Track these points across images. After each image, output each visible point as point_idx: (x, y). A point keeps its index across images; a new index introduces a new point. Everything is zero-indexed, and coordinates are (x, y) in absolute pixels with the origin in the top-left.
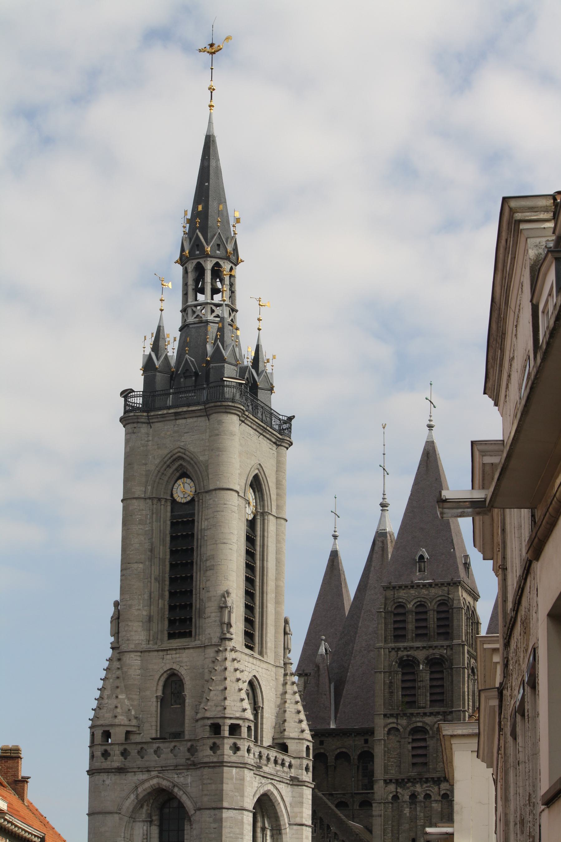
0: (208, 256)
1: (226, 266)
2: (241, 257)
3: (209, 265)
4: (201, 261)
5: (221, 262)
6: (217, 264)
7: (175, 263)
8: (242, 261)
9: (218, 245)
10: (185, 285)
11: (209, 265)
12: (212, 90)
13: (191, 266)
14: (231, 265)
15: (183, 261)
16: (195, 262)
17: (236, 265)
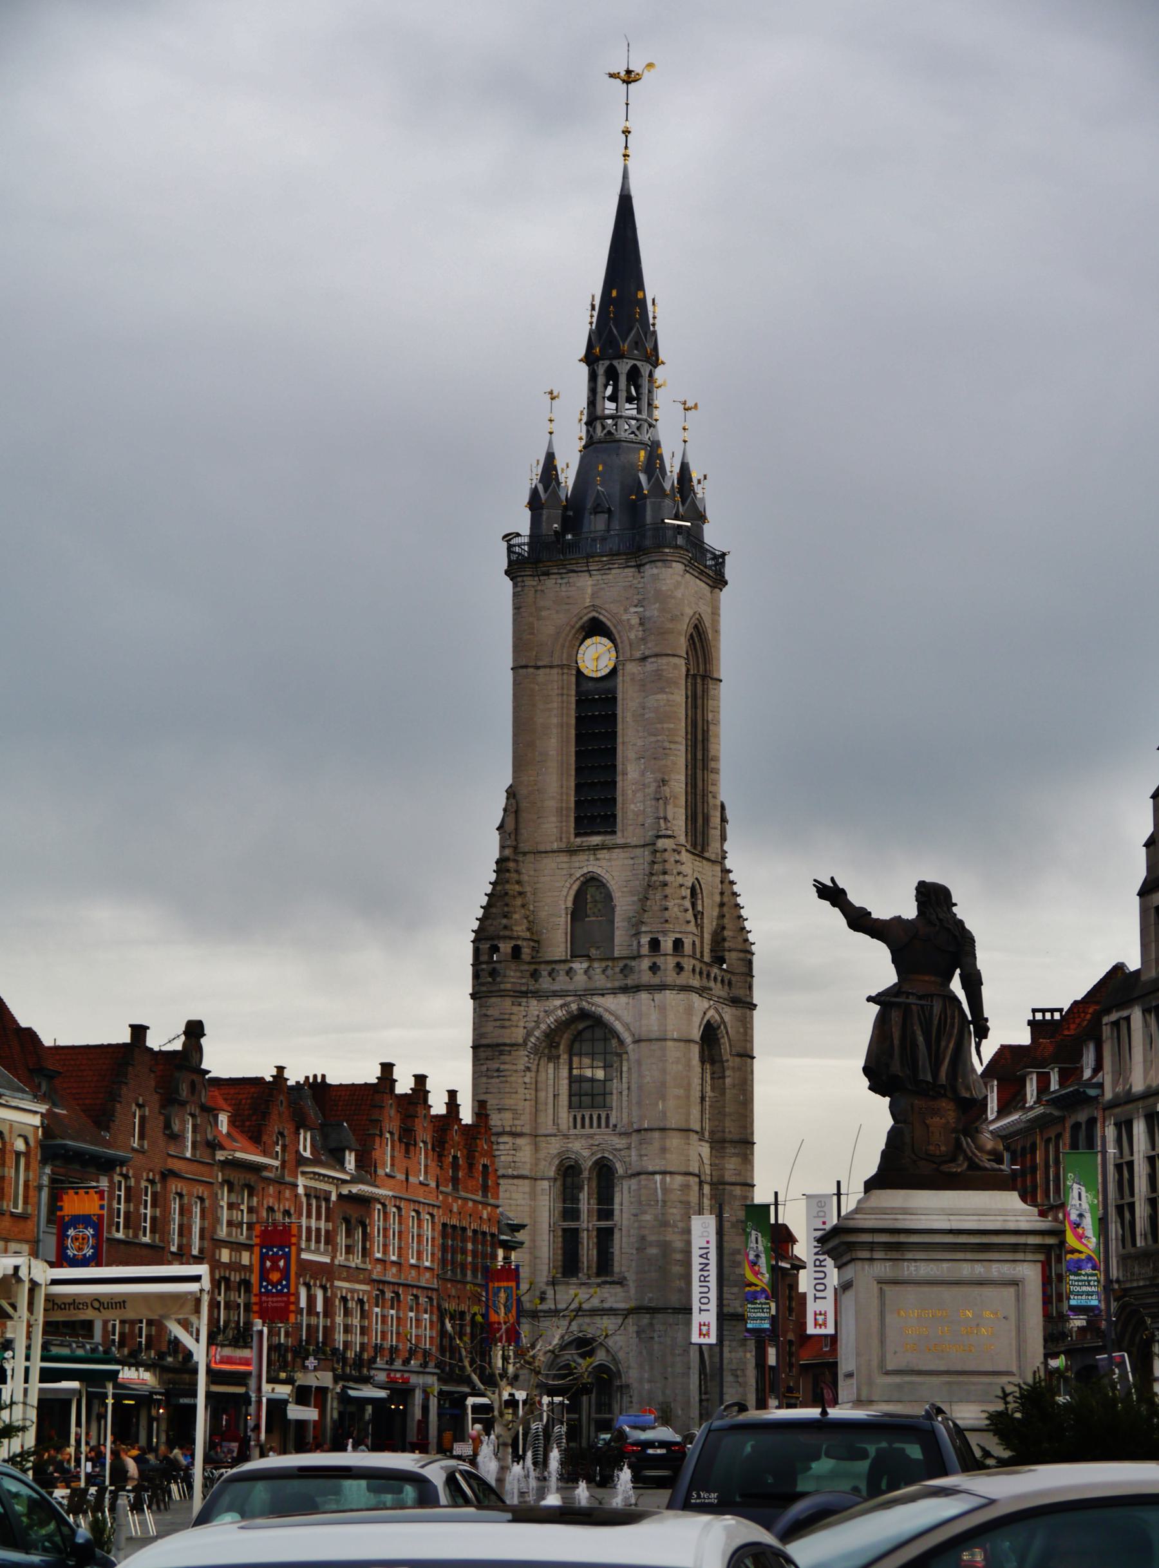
0: (621, 356)
1: (645, 369)
2: (662, 357)
3: (623, 367)
4: (615, 363)
5: (639, 364)
6: (634, 367)
7: (580, 361)
8: (663, 363)
9: (636, 343)
10: (593, 391)
11: (623, 367)
12: (626, 132)
13: (601, 371)
14: (651, 367)
15: (590, 359)
16: (607, 363)
17: (655, 367)
